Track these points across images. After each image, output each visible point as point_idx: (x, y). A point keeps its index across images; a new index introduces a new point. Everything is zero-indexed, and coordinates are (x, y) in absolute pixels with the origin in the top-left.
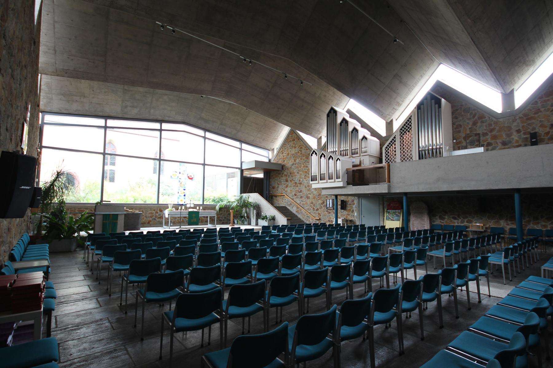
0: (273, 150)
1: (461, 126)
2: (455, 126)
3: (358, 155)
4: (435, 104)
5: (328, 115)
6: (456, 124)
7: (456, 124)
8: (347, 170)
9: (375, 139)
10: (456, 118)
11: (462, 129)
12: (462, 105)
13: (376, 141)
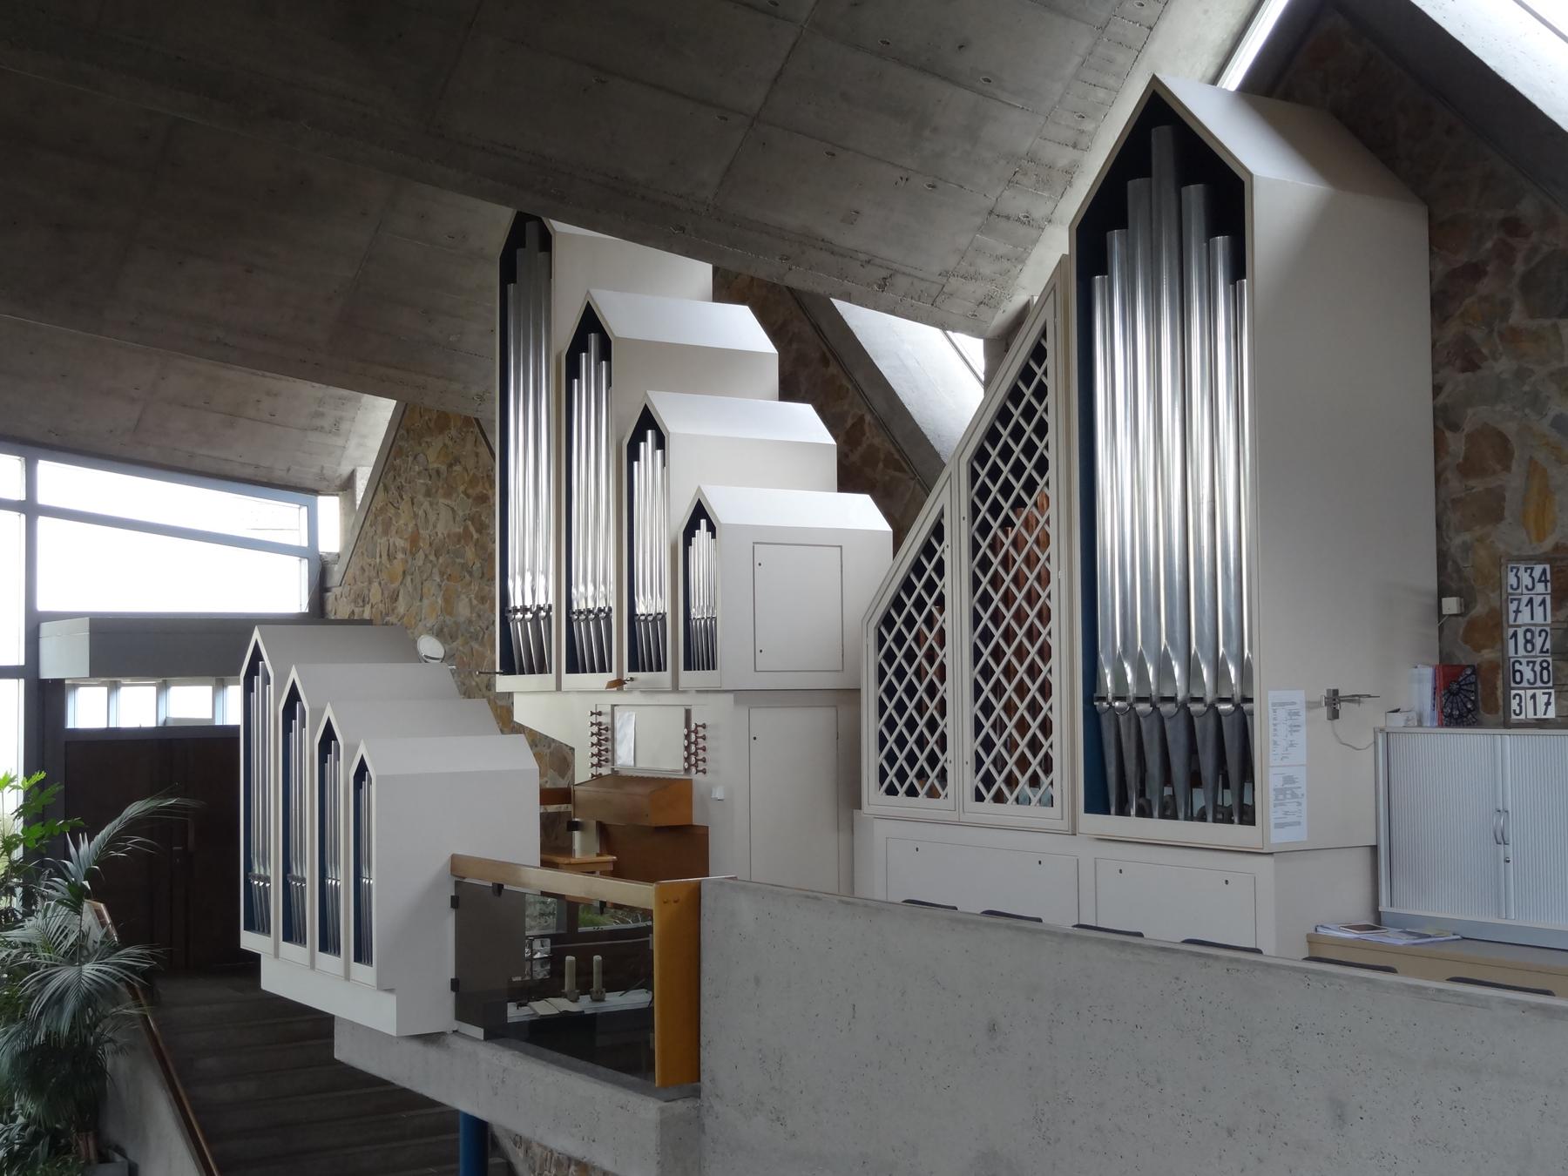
0: (347, 486)
1: (1503, 448)
2: (1457, 444)
3: (665, 677)
4: (1213, 230)
5: (509, 272)
6: (1473, 417)
7: (1473, 417)
8: (457, 865)
9: (862, 514)
10: (1471, 362)
11: (1513, 481)
12: (1513, 226)
13: (838, 543)
